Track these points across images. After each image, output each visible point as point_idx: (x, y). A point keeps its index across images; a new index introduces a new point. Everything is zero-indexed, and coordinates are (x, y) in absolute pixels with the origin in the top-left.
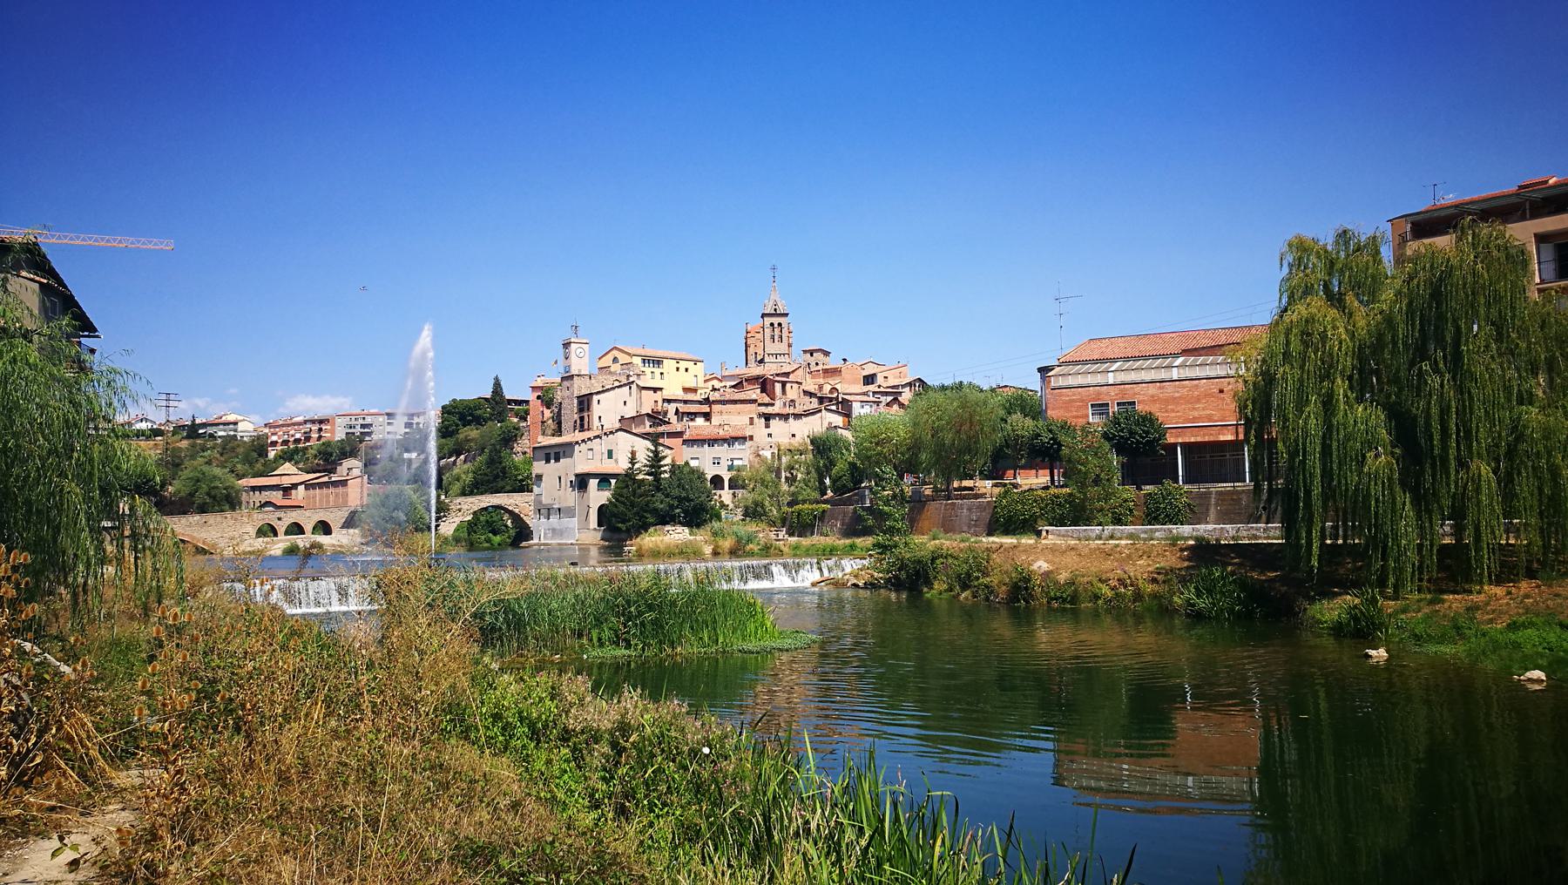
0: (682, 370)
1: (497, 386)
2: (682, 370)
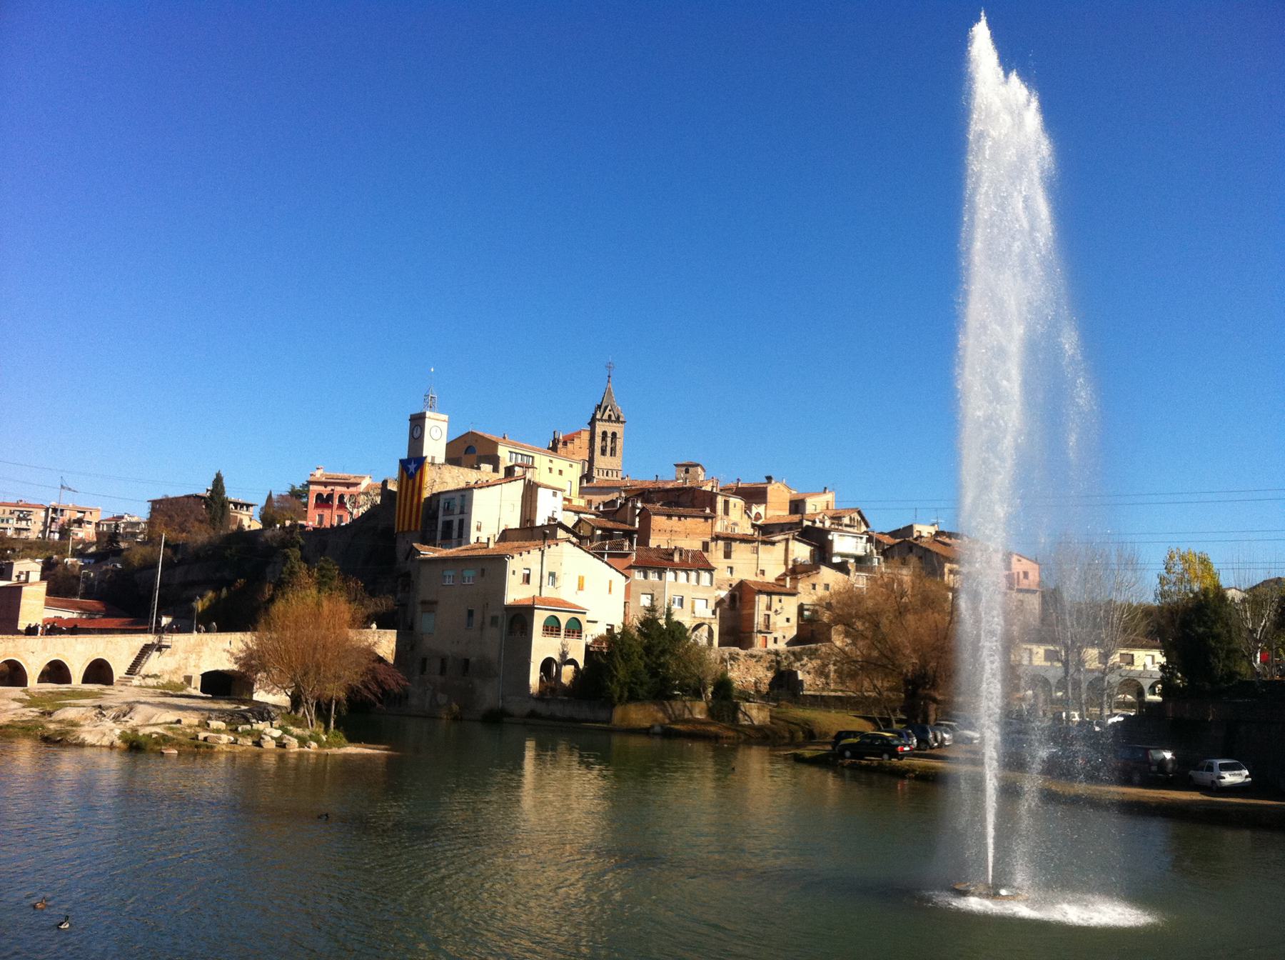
0: (556, 471)
1: (218, 481)
2: (556, 471)
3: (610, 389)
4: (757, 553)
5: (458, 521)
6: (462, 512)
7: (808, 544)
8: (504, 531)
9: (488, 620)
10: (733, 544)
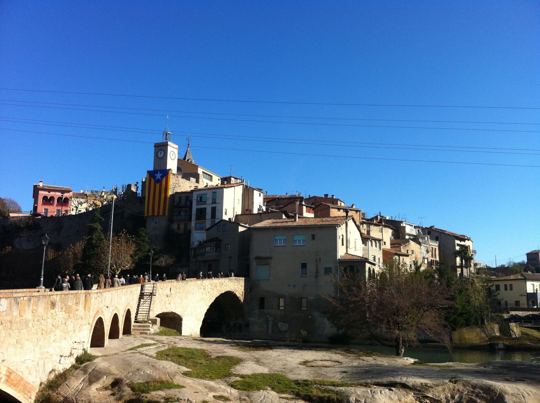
3: (189, 151)
4: (382, 232)
5: (195, 210)
6: (214, 202)
7: (391, 229)
8: (236, 216)
9: (322, 271)
10: (371, 226)
